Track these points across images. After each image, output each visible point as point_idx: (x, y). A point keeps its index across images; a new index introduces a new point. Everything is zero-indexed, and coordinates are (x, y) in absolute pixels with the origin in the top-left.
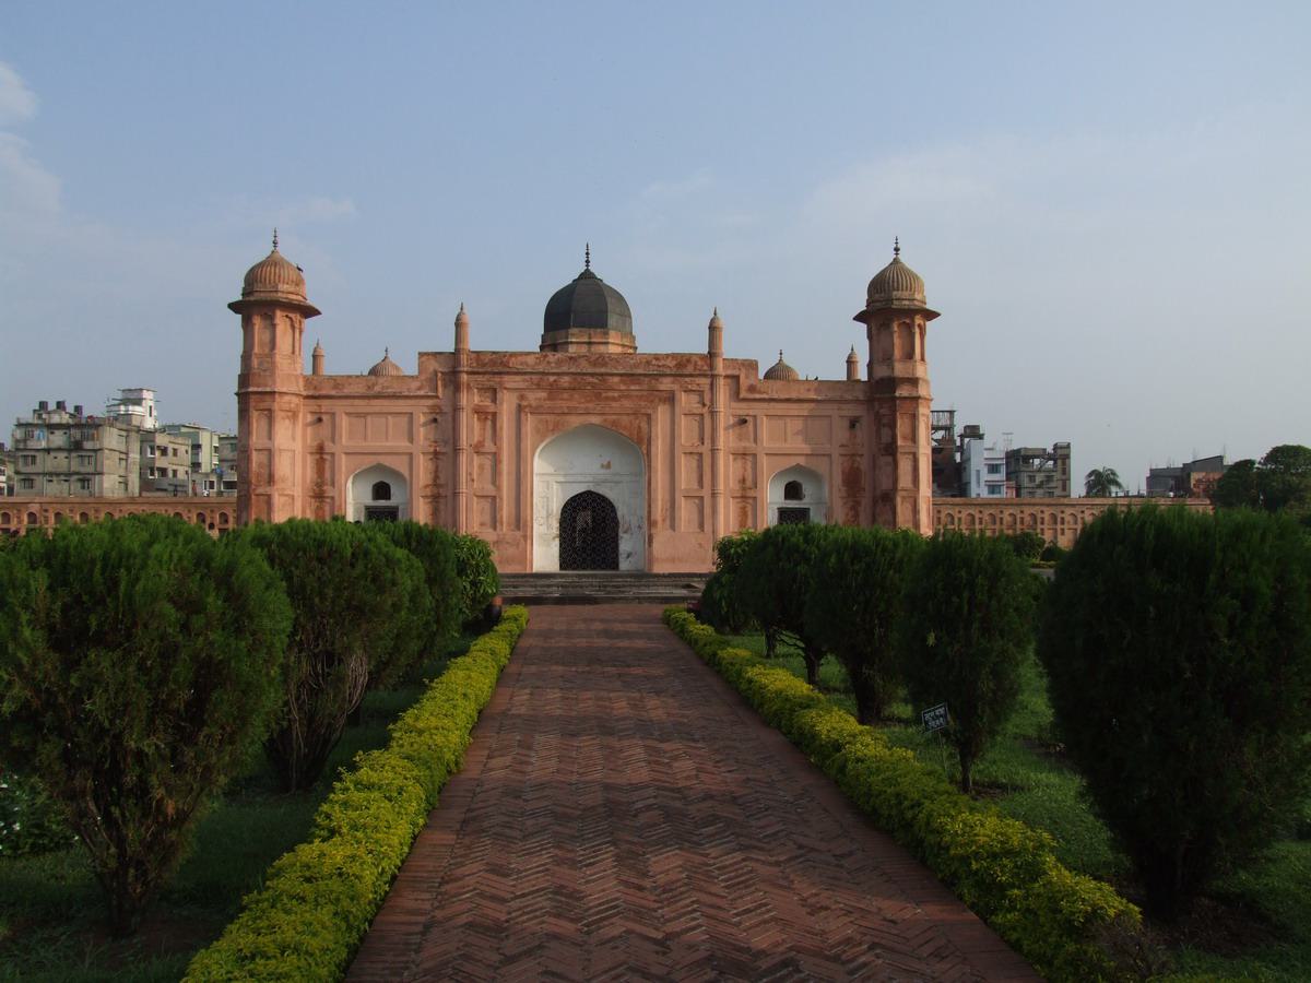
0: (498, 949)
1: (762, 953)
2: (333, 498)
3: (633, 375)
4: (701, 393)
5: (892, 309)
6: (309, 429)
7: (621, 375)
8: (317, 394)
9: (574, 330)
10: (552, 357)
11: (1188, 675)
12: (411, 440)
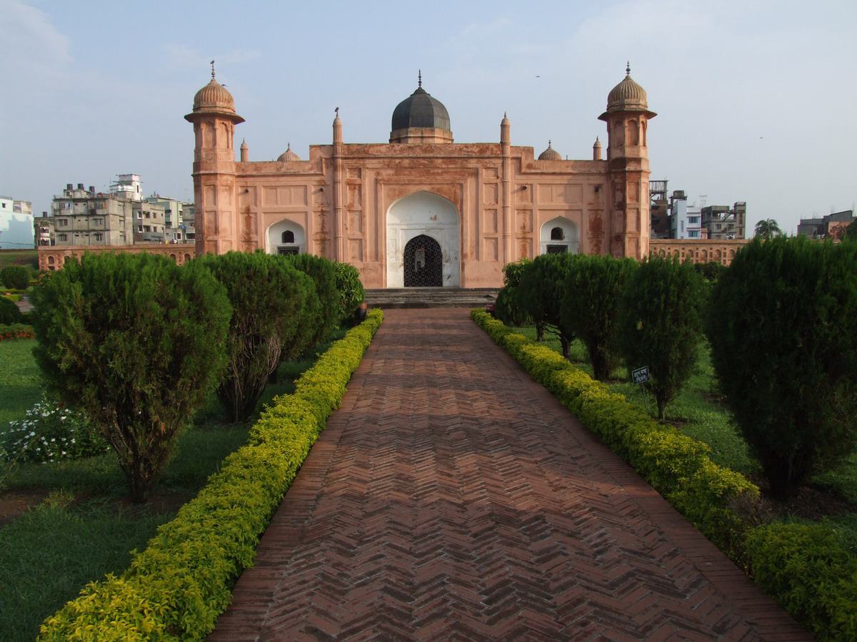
0: (361, 509)
1: (524, 512)
2: (257, 242)
3: (450, 158)
5: (624, 112)
6: (240, 198)
7: (443, 158)
8: (244, 174)
9: (411, 129)
10: (397, 147)
11: (800, 345)
12: (306, 203)
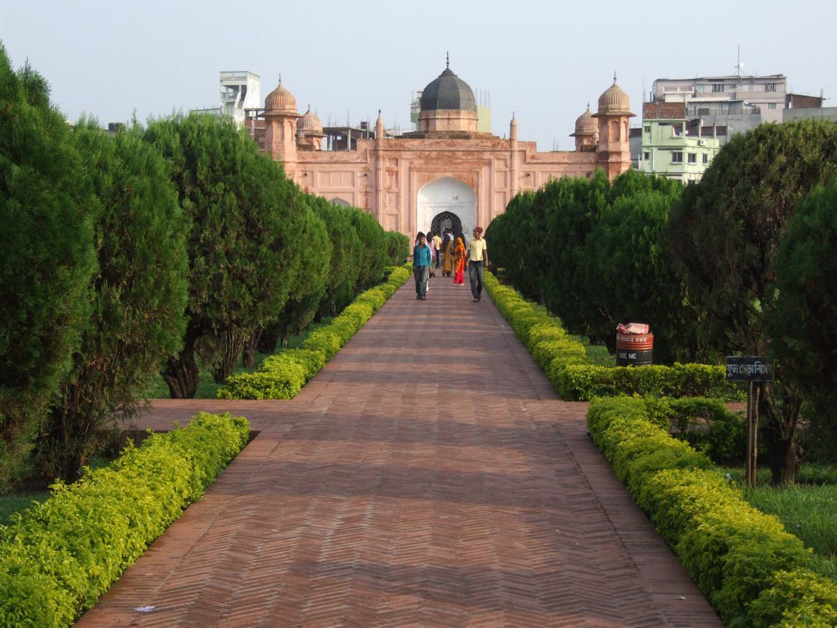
4: (505, 160)
9: (439, 111)
12: (354, 186)
